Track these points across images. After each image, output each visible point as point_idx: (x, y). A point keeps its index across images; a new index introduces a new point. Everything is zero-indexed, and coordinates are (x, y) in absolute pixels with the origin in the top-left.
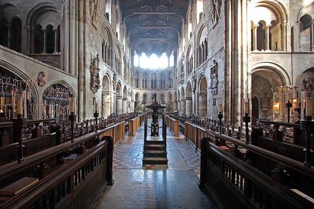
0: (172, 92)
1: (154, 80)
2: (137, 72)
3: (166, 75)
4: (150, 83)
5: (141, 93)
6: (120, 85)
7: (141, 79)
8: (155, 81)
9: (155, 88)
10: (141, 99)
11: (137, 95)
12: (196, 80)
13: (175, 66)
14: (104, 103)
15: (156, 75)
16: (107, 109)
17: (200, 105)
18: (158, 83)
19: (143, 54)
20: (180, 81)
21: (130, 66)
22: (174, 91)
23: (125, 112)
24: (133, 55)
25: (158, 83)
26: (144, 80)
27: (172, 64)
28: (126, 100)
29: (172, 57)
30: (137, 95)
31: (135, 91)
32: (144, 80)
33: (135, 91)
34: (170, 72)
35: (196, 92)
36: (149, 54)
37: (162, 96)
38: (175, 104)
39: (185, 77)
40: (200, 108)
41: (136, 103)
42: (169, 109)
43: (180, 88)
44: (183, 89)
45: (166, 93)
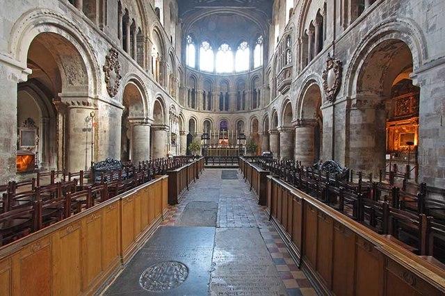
0: (259, 115)
1: (224, 94)
2: (193, 77)
4: (218, 99)
5: (200, 117)
6: (142, 89)
7: (200, 90)
8: (227, 96)
10: (200, 129)
12: (341, 65)
13: (263, 68)
14: (72, 131)
15: (228, 84)
16: (82, 147)
17: (354, 135)
18: (233, 99)
19: (205, 44)
20: (280, 84)
21: (178, 63)
22: (263, 113)
23: (163, 155)
24: (184, 44)
25: (233, 99)
27: (258, 62)
28: (164, 129)
29: (259, 49)
30: (192, 122)
31: (188, 115)
32: (207, 93)
33: (188, 115)
34: (255, 78)
35: (341, 97)
36: (216, 45)
37: (240, 123)
38: (265, 138)
39: (295, 73)
40: (353, 145)
41: (190, 138)
42: (253, 148)
43: (278, 105)
44: (287, 105)
45: (247, 117)
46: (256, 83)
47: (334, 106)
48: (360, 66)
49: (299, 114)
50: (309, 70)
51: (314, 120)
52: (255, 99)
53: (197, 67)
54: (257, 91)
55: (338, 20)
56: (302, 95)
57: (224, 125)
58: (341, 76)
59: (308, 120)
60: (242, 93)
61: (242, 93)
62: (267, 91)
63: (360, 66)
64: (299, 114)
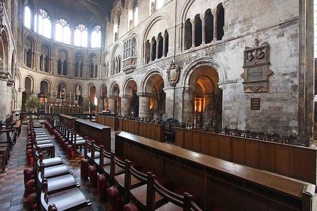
0: (97, 84)
1: (62, 61)
3: (86, 58)
5: (38, 77)
7: (38, 53)
8: (66, 63)
9: (65, 74)
10: (36, 88)
11: (28, 80)
12: (179, 70)
17: (186, 105)
18: (71, 67)
26: (44, 57)
30: (28, 80)
32: (44, 57)
33: (24, 72)
45: (85, 84)
46: (94, 59)
47: (174, 89)
48: (191, 72)
49: (143, 89)
50: (154, 65)
51: (151, 94)
52: (92, 71)
53: (32, 30)
54: (94, 65)
55: (177, 45)
56: (146, 78)
57: (61, 87)
58: (180, 74)
59: (148, 93)
60: (80, 64)
61: (80, 64)
62: (104, 67)
63: (191, 72)
64: (143, 89)
